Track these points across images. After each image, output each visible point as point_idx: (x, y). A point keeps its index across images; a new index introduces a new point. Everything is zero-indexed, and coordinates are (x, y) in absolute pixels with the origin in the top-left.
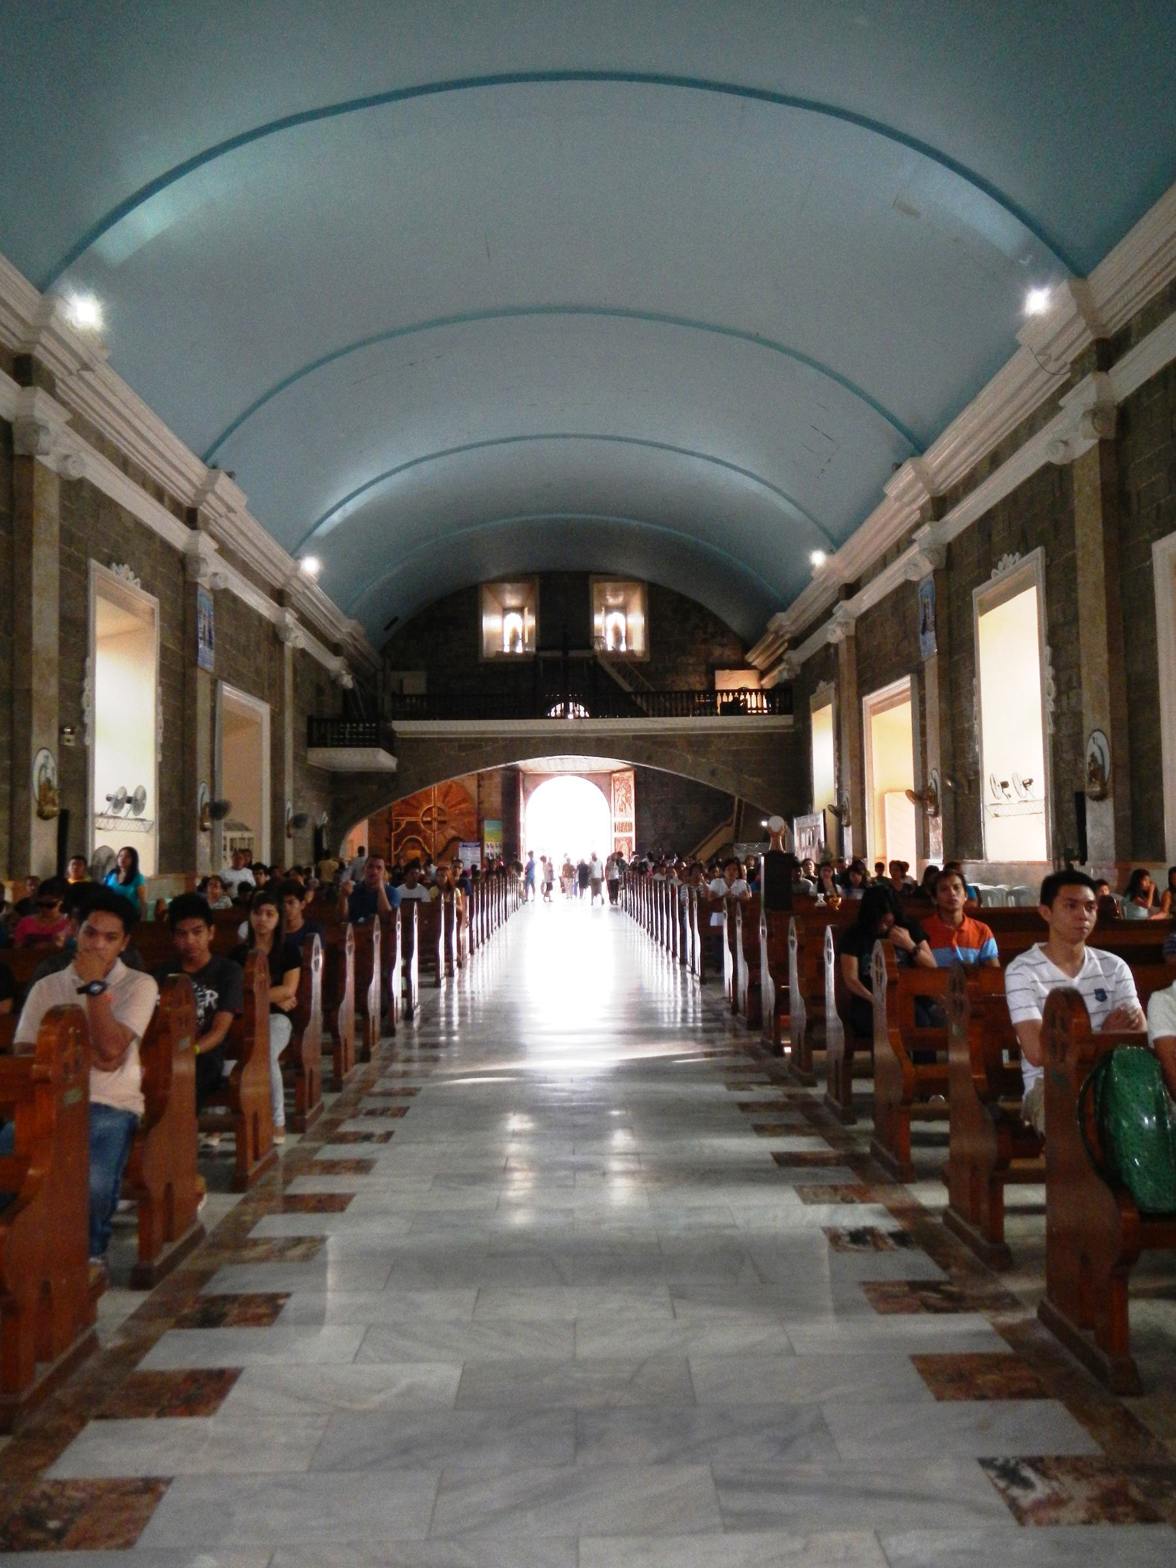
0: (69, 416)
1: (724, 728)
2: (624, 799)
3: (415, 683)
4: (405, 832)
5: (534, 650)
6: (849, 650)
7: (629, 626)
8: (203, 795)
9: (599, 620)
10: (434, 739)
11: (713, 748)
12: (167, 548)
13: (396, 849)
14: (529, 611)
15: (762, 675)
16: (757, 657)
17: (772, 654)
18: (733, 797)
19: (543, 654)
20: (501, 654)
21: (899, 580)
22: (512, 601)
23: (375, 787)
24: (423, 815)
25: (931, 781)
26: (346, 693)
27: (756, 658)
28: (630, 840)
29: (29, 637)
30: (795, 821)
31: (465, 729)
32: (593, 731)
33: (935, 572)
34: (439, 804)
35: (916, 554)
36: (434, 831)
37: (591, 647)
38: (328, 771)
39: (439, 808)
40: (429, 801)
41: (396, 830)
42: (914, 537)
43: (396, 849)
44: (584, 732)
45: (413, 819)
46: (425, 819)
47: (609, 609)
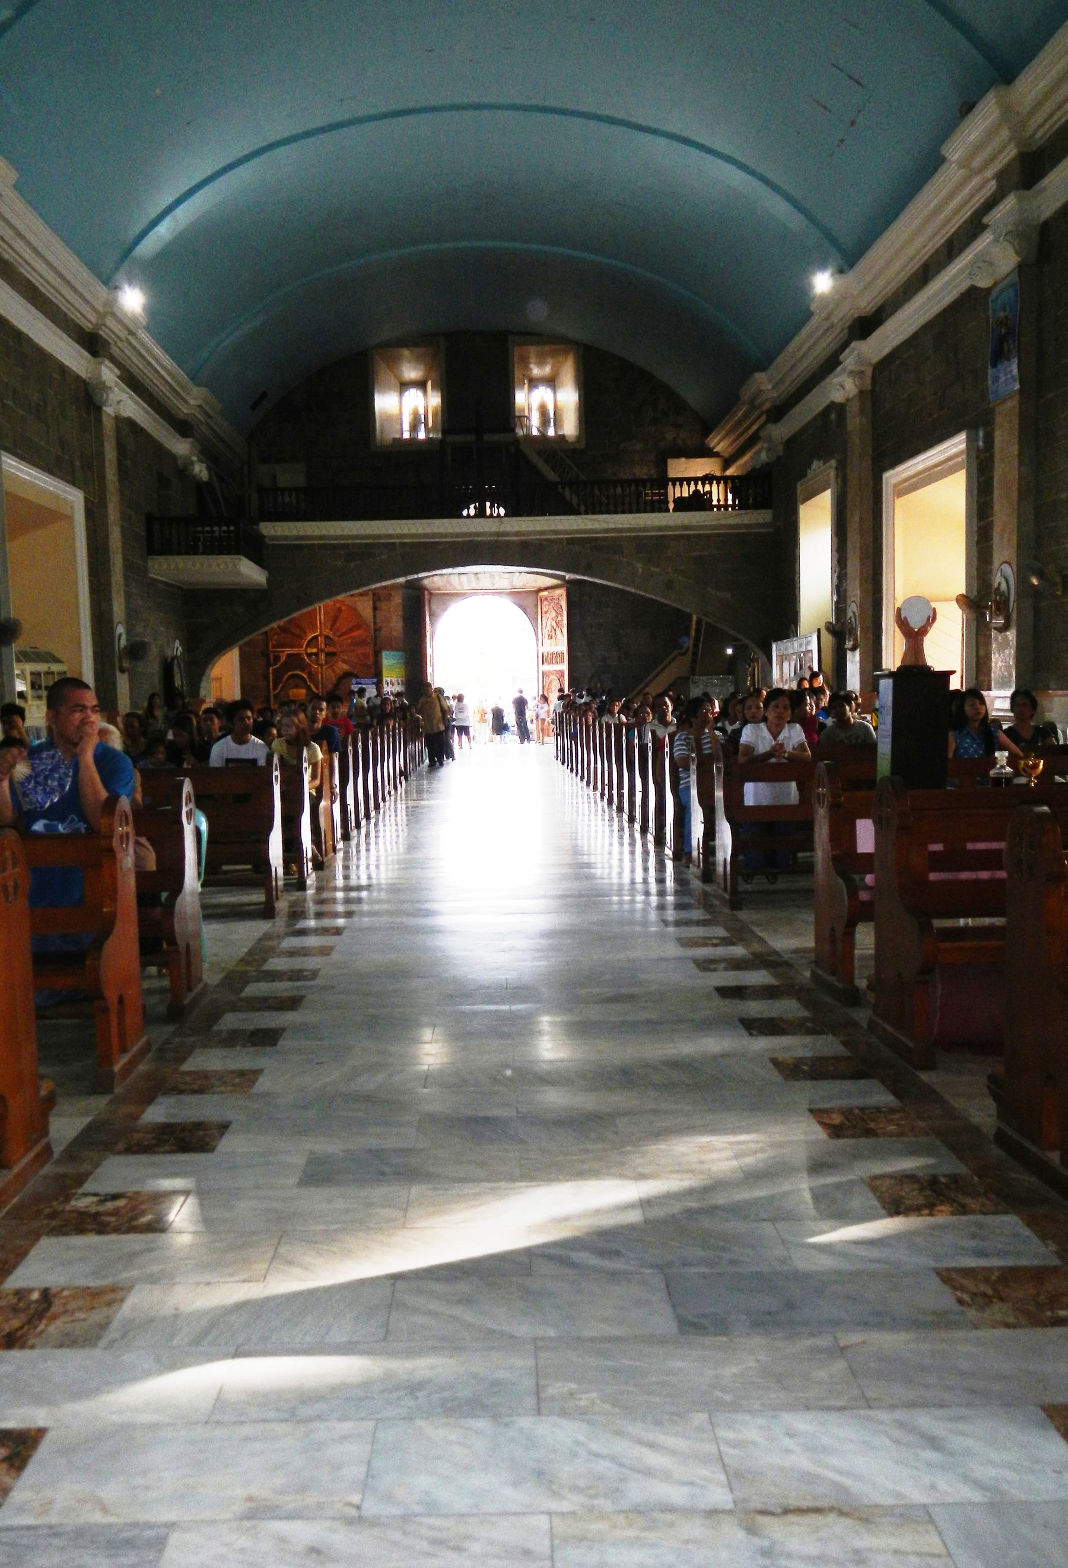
2: (554, 624)
4: (286, 667)
5: (440, 436)
6: (862, 411)
7: (559, 404)
9: (521, 397)
11: (669, 554)
13: (275, 688)
14: (433, 387)
15: (727, 464)
16: (718, 443)
17: (741, 435)
18: (690, 616)
19: (450, 439)
20: (399, 442)
21: (964, 287)
22: (411, 373)
24: (307, 646)
25: (997, 580)
26: (200, 487)
27: (720, 443)
28: (562, 673)
32: (517, 534)
33: (1021, 268)
34: (326, 632)
35: (989, 244)
36: (321, 666)
37: (513, 430)
38: (179, 588)
39: (327, 637)
40: (314, 630)
42: (985, 220)
43: (275, 688)
45: (295, 651)
46: (309, 651)
47: (533, 383)
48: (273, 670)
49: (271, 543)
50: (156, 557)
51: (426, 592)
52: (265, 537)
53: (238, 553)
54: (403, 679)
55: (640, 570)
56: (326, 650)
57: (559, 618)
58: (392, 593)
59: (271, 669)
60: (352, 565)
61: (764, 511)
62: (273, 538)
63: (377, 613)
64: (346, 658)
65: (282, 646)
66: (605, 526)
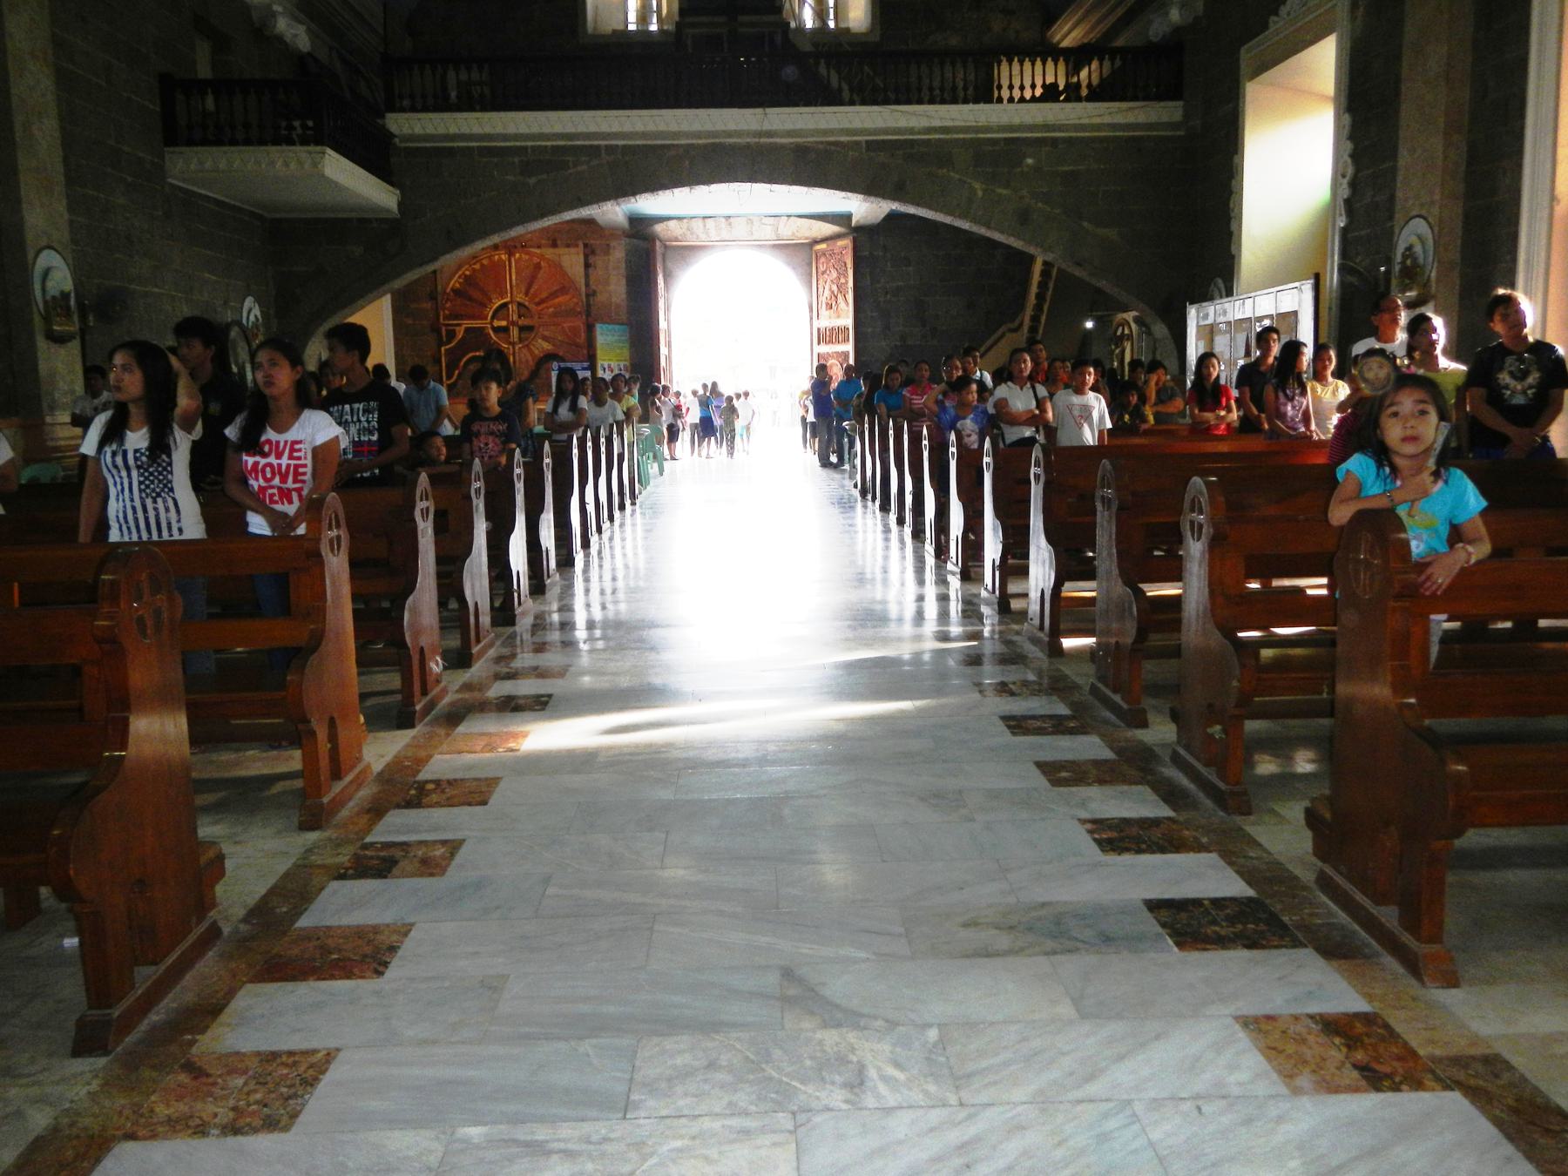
1: (1047, 127)
2: (835, 288)
4: (464, 346)
10: (473, 147)
24: (493, 318)
28: (846, 355)
30: (1192, 313)
31: (535, 130)
32: (790, 133)
34: (520, 298)
36: (513, 344)
38: (260, 217)
39: (520, 304)
40: (502, 295)
41: (449, 342)
43: (449, 377)
44: (769, 134)
46: (496, 323)
48: (446, 350)
49: (403, 145)
50: (177, 149)
51: (658, 243)
52: (395, 136)
53: (319, 141)
54: (627, 363)
55: (980, 193)
56: (520, 323)
57: (843, 280)
58: (613, 244)
59: (443, 349)
60: (532, 181)
61: (1171, 104)
63: (591, 270)
64: (546, 333)
65: (457, 317)
66: (924, 123)
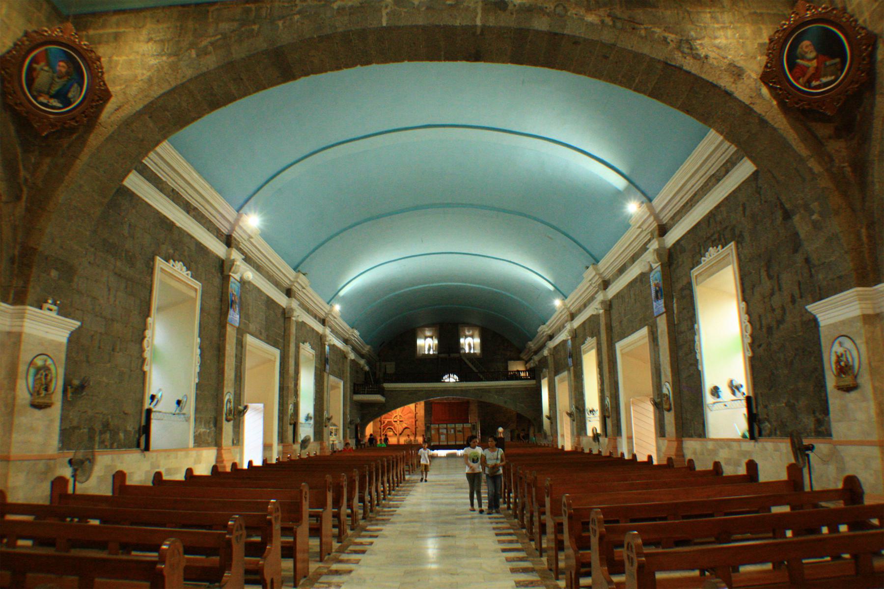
0: (298, 303)
3: (391, 367)
4: (387, 425)
8: (326, 415)
9: (462, 341)
12: (317, 333)
15: (526, 362)
20: (425, 355)
22: (428, 333)
23: (377, 409)
26: (366, 373)
29: (288, 370)
34: (400, 414)
37: (459, 353)
46: (395, 420)
47: (466, 337)
52: (384, 388)
62: (388, 388)
